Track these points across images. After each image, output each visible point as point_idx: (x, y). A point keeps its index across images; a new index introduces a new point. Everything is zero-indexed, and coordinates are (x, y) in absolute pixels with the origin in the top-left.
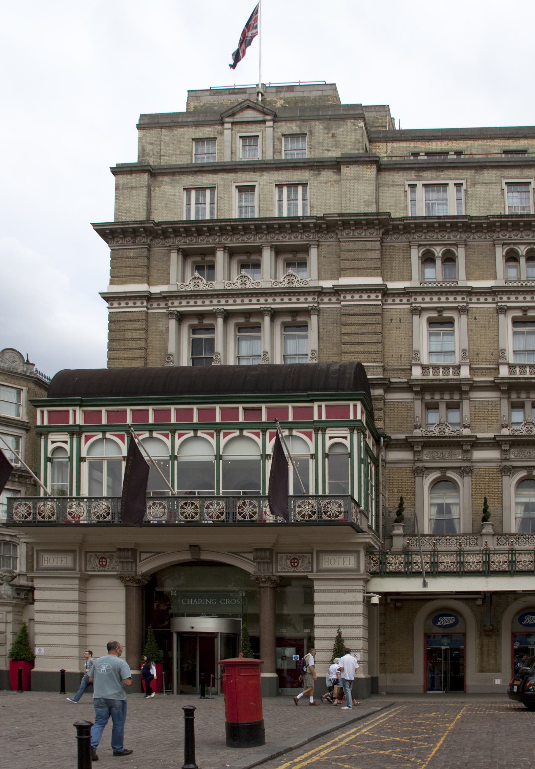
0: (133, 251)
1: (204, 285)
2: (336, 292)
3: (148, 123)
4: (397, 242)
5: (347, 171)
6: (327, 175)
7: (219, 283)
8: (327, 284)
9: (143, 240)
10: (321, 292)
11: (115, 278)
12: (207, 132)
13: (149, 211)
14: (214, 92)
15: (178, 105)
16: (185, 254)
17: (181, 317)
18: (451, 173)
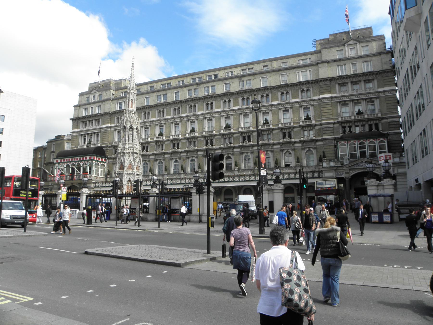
0: (76, 122)
1: (85, 129)
2: (103, 128)
3: (81, 95)
4: (113, 116)
5: (107, 102)
6: (104, 103)
7: (88, 128)
8: (101, 127)
9: (77, 121)
10: (100, 128)
11: (73, 128)
12: (88, 96)
13: (78, 114)
14: (93, 83)
15: (86, 89)
16: (83, 122)
17: (82, 135)
18: (123, 99)
